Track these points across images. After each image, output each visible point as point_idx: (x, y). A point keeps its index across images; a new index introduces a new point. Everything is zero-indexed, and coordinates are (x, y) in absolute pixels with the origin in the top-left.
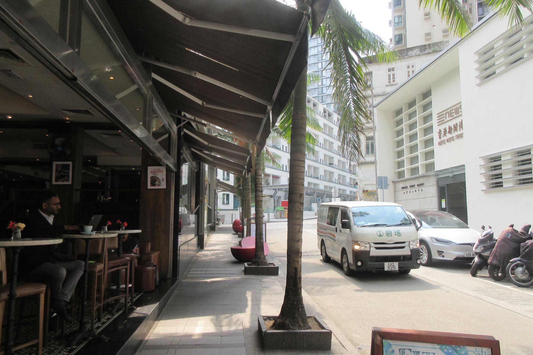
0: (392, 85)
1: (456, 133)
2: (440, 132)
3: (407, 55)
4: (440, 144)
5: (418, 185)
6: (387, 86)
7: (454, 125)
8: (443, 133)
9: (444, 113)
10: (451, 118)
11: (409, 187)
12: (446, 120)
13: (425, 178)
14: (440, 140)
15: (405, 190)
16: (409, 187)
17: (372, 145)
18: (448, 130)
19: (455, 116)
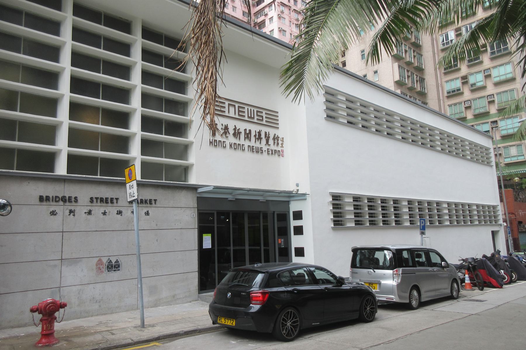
1: (247, 143)
2: (213, 127)
4: (214, 143)
7: (245, 130)
8: (222, 131)
9: (227, 103)
10: (237, 116)
12: (226, 114)
15: (60, 208)
18: (231, 131)
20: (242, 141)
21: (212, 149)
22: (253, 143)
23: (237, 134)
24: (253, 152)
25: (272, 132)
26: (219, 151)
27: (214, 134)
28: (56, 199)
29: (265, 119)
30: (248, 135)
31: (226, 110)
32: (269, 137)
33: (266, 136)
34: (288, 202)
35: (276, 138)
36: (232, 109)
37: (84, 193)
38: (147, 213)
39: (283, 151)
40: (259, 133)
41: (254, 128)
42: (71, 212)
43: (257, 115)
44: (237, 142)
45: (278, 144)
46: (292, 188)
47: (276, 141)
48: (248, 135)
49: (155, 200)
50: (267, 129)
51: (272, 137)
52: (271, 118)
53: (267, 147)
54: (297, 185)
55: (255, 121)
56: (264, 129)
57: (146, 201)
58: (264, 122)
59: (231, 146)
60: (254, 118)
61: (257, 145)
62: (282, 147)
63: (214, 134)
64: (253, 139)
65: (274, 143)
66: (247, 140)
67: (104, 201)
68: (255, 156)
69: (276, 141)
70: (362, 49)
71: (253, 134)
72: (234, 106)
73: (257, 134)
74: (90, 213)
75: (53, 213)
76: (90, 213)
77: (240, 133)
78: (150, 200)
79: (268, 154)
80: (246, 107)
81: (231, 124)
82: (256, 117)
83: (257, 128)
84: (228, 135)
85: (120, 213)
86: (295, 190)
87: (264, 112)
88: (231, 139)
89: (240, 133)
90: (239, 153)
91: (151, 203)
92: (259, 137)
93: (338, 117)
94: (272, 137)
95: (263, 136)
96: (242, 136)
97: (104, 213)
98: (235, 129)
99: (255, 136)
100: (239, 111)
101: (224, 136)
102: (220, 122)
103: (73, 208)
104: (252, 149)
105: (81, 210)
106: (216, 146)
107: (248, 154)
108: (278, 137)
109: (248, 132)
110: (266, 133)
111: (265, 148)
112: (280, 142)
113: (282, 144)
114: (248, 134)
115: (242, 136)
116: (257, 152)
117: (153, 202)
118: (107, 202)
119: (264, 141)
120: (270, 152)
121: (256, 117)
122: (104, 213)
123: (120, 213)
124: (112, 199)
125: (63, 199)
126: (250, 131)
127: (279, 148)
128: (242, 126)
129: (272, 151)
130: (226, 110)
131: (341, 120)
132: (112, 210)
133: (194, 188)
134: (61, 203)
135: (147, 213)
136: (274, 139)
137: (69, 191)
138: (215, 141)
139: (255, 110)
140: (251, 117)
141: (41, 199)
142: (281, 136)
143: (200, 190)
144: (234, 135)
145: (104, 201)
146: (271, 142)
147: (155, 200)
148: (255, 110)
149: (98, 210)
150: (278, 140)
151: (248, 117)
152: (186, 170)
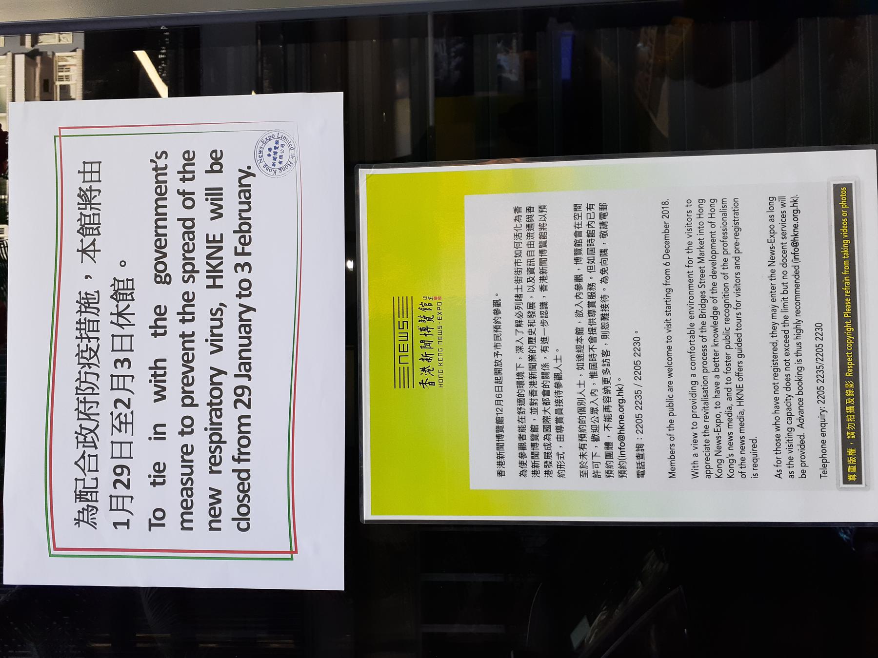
10: (410, 353)
18: (425, 364)
19: (410, 342)
25: (418, 313)
27: (433, 384)
33: (424, 321)
35: (424, 307)
45: (430, 305)
51: (423, 313)
64: (428, 338)
73: (423, 332)
82: (405, 330)
94: (423, 313)
95: (423, 325)
96: (428, 351)
109: (423, 344)
119: (428, 324)
146: (428, 314)
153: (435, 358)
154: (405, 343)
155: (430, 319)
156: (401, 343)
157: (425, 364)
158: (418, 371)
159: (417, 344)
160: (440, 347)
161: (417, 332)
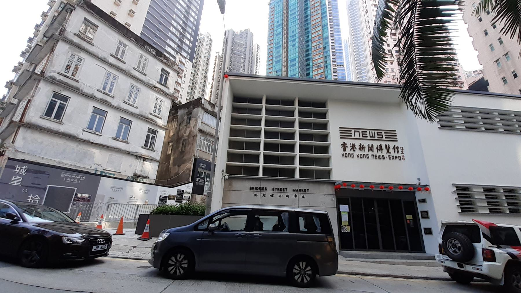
0: (118, 59)
1: (370, 153)
2: (344, 145)
3: (143, 46)
4: (345, 156)
5: (294, 191)
6: (111, 55)
9: (353, 131)
10: (361, 137)
11: (270, 189)
12: (353, 137)
13: (311, 185)
14: (345, 153)
15: (258, 193)
16: (270, 189)
17: (62, 108)
18: (357, 147)
19: (369, 138)
20: (366, 152)
21: (344, 158)
22: (375, 152)
23: (362, 148)
24: (376, 158)
25: (392, 144)
26: (349, 159)
27: (345, 150)
28: (257, 189)
29: (384, 137)
30: (371, 148)
31: (353, 135)
32: (389, 148)
34: (414, 193)
35: (396, 148)
36: (357, 134)
37: (270, 186)
38: (303, 197)
39: (403, 156)
40: (381, 146)
41: (376, 144)
42: (264, 195)
43: (378, 135)
44: (363, 153)
45: (398, 152)
46: (415, 182)
47: (396, 150)
48: (371, 148)
49: (308, 190)
50: (387, 143)
52: (391, 135)
53: (388, 154)
54: (419, 179)
55: (376, 138)
56: (384, 144)
57: (302, 190)
58: (384, 139)
59: (358, 156)
60: (375, 137)
61: (380, 153)
62: (402, 153)
63: (345, 150)
65: (395, 151)
66: (370, 152)
67: (279, 190)
68: (378, 160)
69: (396, 150)
70: (502, 76)
71: (375, 147)
72: (359, 132)
74: (272, 196)
75: (256, 195)
76: (272, 196)
77: (364, 148)
78: (305, 190)
79: (390, 159)
80: (368, 131)
81: (357, 143)
82: (377, 136)
83: (379, 143)
84: (355, 149)
85: (288, 196)
86: (418, 184)
87: (383, 132)
88: (358, 152)
89: (364, 148)
90: (364, 160)
91: (305, 192)
92: (380, 148)
93: (455, 126)
97: (280, 196)
98: (360, 145)
99: (377, 148)
100: (362, 134)
101: (352, 150)
102: (349, 142)
103: (264, 193)
104: (375, 157)
105: (268, 195)
106: (346, 157)
107: (372, 160)
108: (397, 148)
109: (370, 146)
110: (386, 146)
111: (386, 155)
112: (400, 150)
113: (402, 152)
114: (371, 148)
115: (366, 149)
116: (380, 158)
117: (307, 191)
118: (281, 191)
119: (385, 151)
120: (392, 158)
121: (377, 136)
122: (280, 196)
123: (288, 196)
124: (284, 189)
125: (260, 188)
126: (372, 145)
127: (400, 154)
128: (365, 143)
129: (393, 157)
130: (353, 135)
131: (458, 127)
132: (284, 195)
133: (333, 183)
134: (259, 190)
135: (303, 197)
136: (394, 148)
137: (263, 185)
138: (346, 154)
139: (376, 132)
140: (372, 137)
141: (250, 188)
142: (400, 146)
143: (336, 184)
144: (360, 149)
145: (279, 190)
146: (391, 150)
147: (308, 190)
148: (376, 132)
149: (276, 194)
150: (398, 149)
151: (370, 137)
152: (329, 172)
153: (363, 153)
154: (368, 135)
155: (388, 151)
156: (368, 133)
157: (357, 147)
158: (352, 142)
159: (371, 143)
160: (370, 156)
161: (379, 143)
